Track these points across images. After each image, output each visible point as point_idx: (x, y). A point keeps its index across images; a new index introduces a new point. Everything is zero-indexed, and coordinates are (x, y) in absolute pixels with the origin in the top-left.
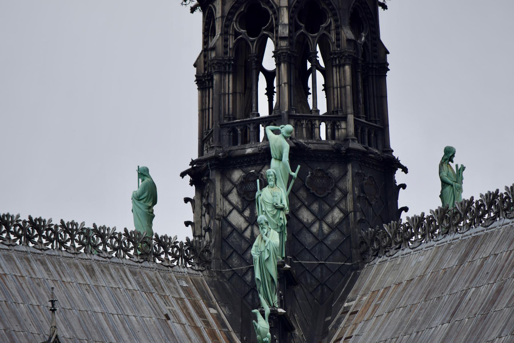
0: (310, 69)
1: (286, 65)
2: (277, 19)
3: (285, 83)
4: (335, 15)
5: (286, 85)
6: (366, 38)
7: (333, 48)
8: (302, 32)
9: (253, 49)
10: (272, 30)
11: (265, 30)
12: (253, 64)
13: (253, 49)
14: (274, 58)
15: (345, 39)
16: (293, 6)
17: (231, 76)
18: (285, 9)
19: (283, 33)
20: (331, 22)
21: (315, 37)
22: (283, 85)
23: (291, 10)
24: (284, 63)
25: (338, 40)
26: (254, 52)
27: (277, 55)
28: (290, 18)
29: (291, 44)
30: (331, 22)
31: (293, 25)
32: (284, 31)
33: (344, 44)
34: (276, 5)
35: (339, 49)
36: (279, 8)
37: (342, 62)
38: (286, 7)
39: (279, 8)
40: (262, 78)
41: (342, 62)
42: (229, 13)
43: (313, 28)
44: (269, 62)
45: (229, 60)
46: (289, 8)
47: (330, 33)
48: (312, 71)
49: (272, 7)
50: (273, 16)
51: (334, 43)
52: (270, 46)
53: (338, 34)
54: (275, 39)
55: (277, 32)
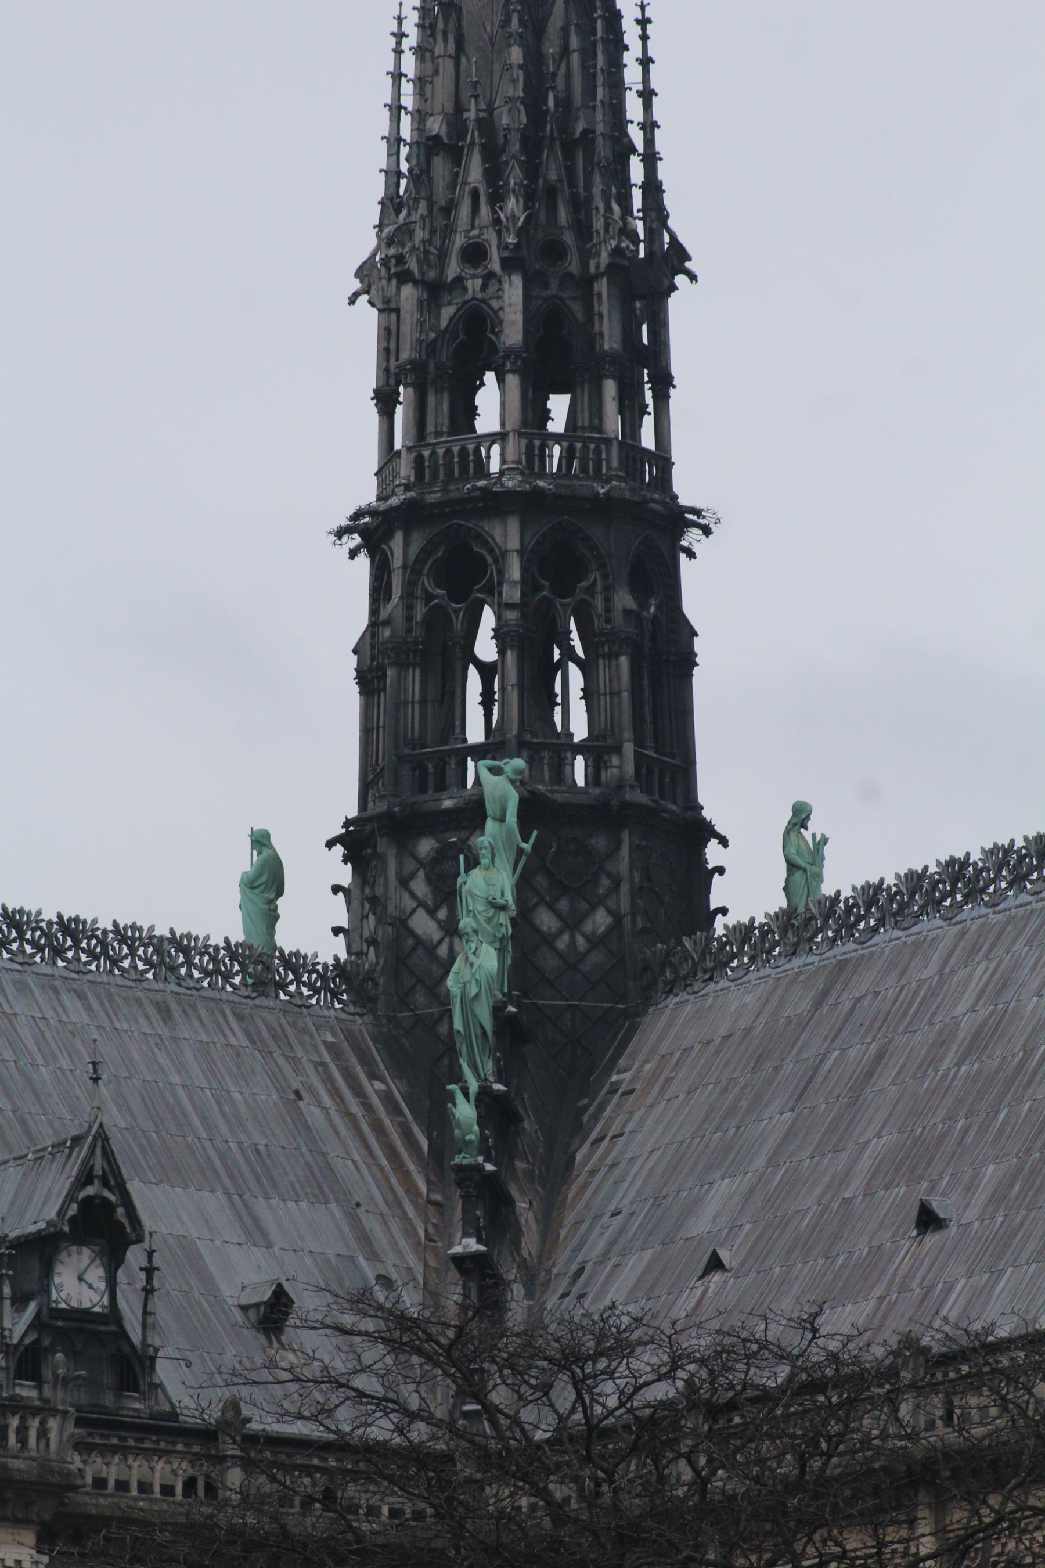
0: (559, 660)
1: (515, 653)
2: (500, 572)
3: (512, 686)
4: (602, 566)
5: (516, 689)
6: (658, 607)
7: (598, 624)
8: (545, 597)
9: (458, 624)
10: (492, 591)
11: (478, 591)
12: (458, 650)
13: (458, 624)
14: (494, 641)
15: (620, 608)
16: (529, 549)
17: (418, 672)
18: (515, 554)
19: (512, 597)
20: (595, 580)
21: (568, 605)
22: (509, 688)
23: (526, 556)
24: (512, 650)
25: (608, 610)
26: (459, 628)
27: (499, 635)
28: (524, 570)
29: (524, 616)
30: (595, 580)
31: (528, 583)
32: (513, 594)
33: (618, 618)
34: (499, 548)
35: (609, 627)
36: (504, 553)
37: (615, 648)
38: (517, 551)
39: (504, 553)
40: (473, 672)
41: (615, 648)
42: (417, 560)
43: (564, 589)
44: (486, 648)
45: (416, 642)
46: (521, 553)
47: (593, 598)
48: (562, 665)
49: (491, 551)
50: (493, 567)
51: (601, 615)
52: (488, 619)
53: (608, 600)
54: (496, 608)
55: (500, 594)
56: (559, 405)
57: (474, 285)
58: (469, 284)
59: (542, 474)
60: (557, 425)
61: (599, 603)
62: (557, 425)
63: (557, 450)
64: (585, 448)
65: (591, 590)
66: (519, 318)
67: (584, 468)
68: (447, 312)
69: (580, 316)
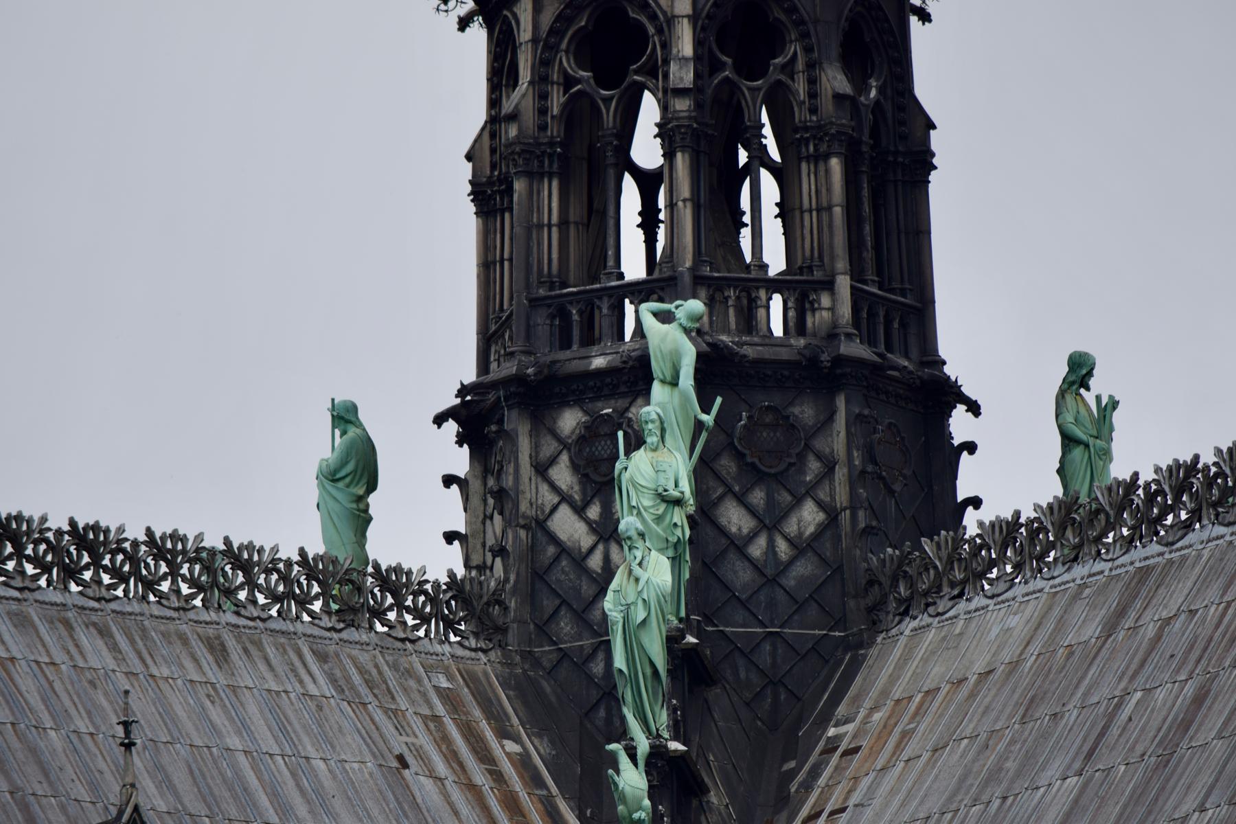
0: (746, 165)
1: (687, 156)
2: (665, 46)
3: (684, 201)
4: (805, 36)
5: (689, 204)
6: (881, 90)
7: (801, 115)
8: (727, 78)
9: (609, 117)
10: (655, 71)
11: (636, 72)
12: (609, 154)
13: (609, 117)
14: (659, 140)
15: (830, 93)
16: (704, 15)
17: (555, 183)
18: (685, 21)
19: (681, 79)
20: (795, 53)
21: (758, 89)
22: (680, 204)
23: (700, 23)
24: (683, 152)
25: (813, 95)
26: (611, 125)
27: (665, 132)
28: (698, 43)
29: (699, 105)
30: (795, 53)
31: (704, 60)
32: (682, 75)
33: (827, 105)
34: (664, 13)
35: (814, 118)
36: (671, 20)
37: (823, 148)
38: (688, 16)
39: (671, 20)
40: (630, 187)
41: (823, 148)
42: (551, 31)
43: (752, 67)
44: (646, 150)
45: (552, 144)
46: (694, 18)
47: (793, 79)
48: (750, 170)
49: (653, 17)
50: (656, 38)
51: (804, 102)
52: (649, 110)
53: (812, 81)
54: (660, 95)
55: (666, 76)
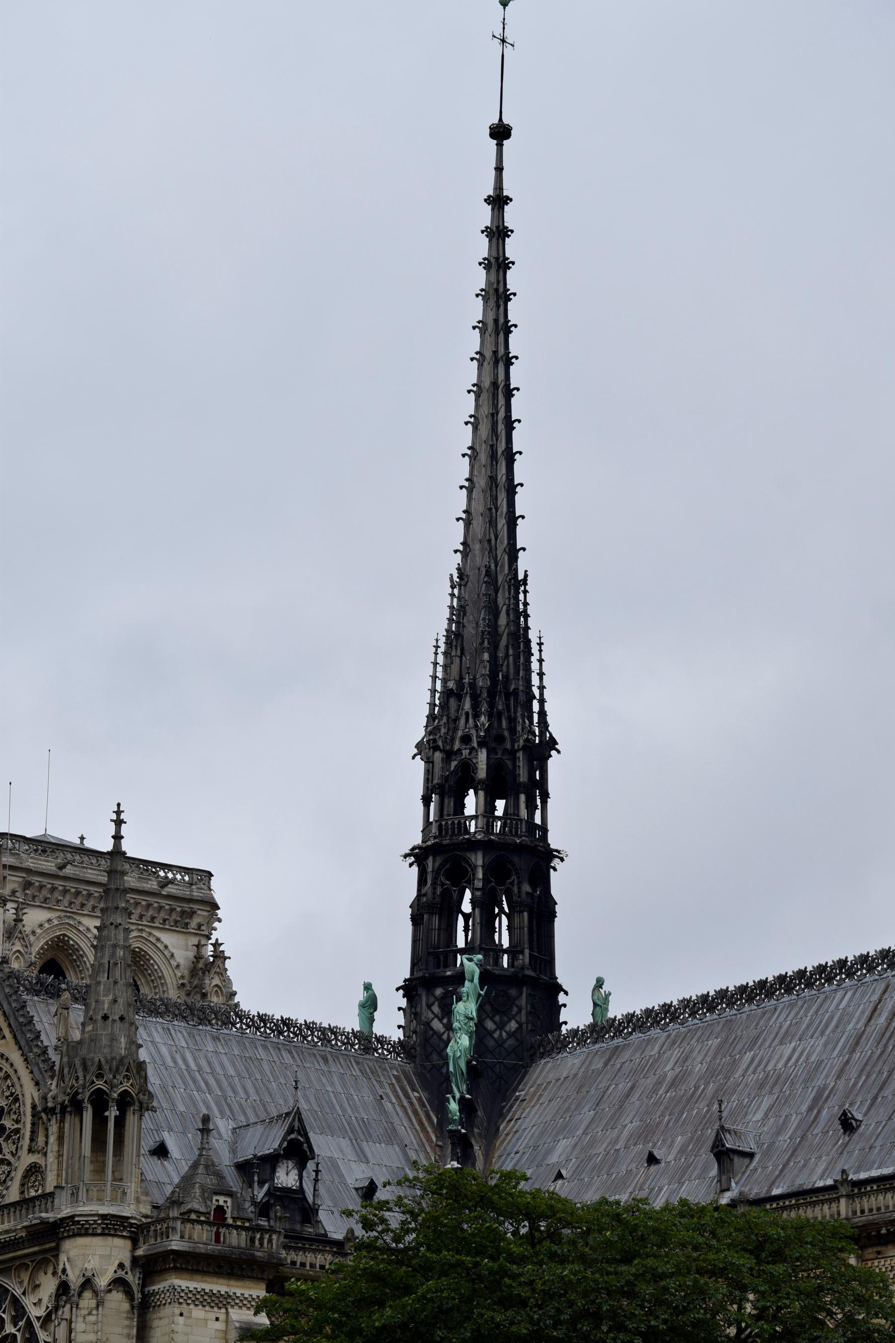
2: (474, 875)
4: (517, 873)
7: (515, 898)
25: (519, 892)
27: (473, 901)
28: (484, 874)
29: (483, 894)
31: (485, 879)
33: (524, 896)
36: (476, 867)
39: (476, 867)
40: (460, 917)
42: (438, 869)
44: (466, 907)
46: (483, 866)
48: (499, 915)
49: (470, 866)
52: (468, 894)
53: (519, 888)
56: (500, 804)
57: (465, 752)
58: (464, 752)
59: (493, 834)
60: (499, 812)
61: (516, 890)
62: (499, 812)
63: (499, 823)
64: (511, 822)
65: (512, 883)
66: (485, 767)
67: (511, 831)
68: (454, 764)
69: (510, 767)
